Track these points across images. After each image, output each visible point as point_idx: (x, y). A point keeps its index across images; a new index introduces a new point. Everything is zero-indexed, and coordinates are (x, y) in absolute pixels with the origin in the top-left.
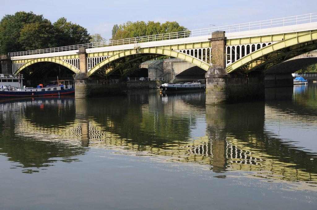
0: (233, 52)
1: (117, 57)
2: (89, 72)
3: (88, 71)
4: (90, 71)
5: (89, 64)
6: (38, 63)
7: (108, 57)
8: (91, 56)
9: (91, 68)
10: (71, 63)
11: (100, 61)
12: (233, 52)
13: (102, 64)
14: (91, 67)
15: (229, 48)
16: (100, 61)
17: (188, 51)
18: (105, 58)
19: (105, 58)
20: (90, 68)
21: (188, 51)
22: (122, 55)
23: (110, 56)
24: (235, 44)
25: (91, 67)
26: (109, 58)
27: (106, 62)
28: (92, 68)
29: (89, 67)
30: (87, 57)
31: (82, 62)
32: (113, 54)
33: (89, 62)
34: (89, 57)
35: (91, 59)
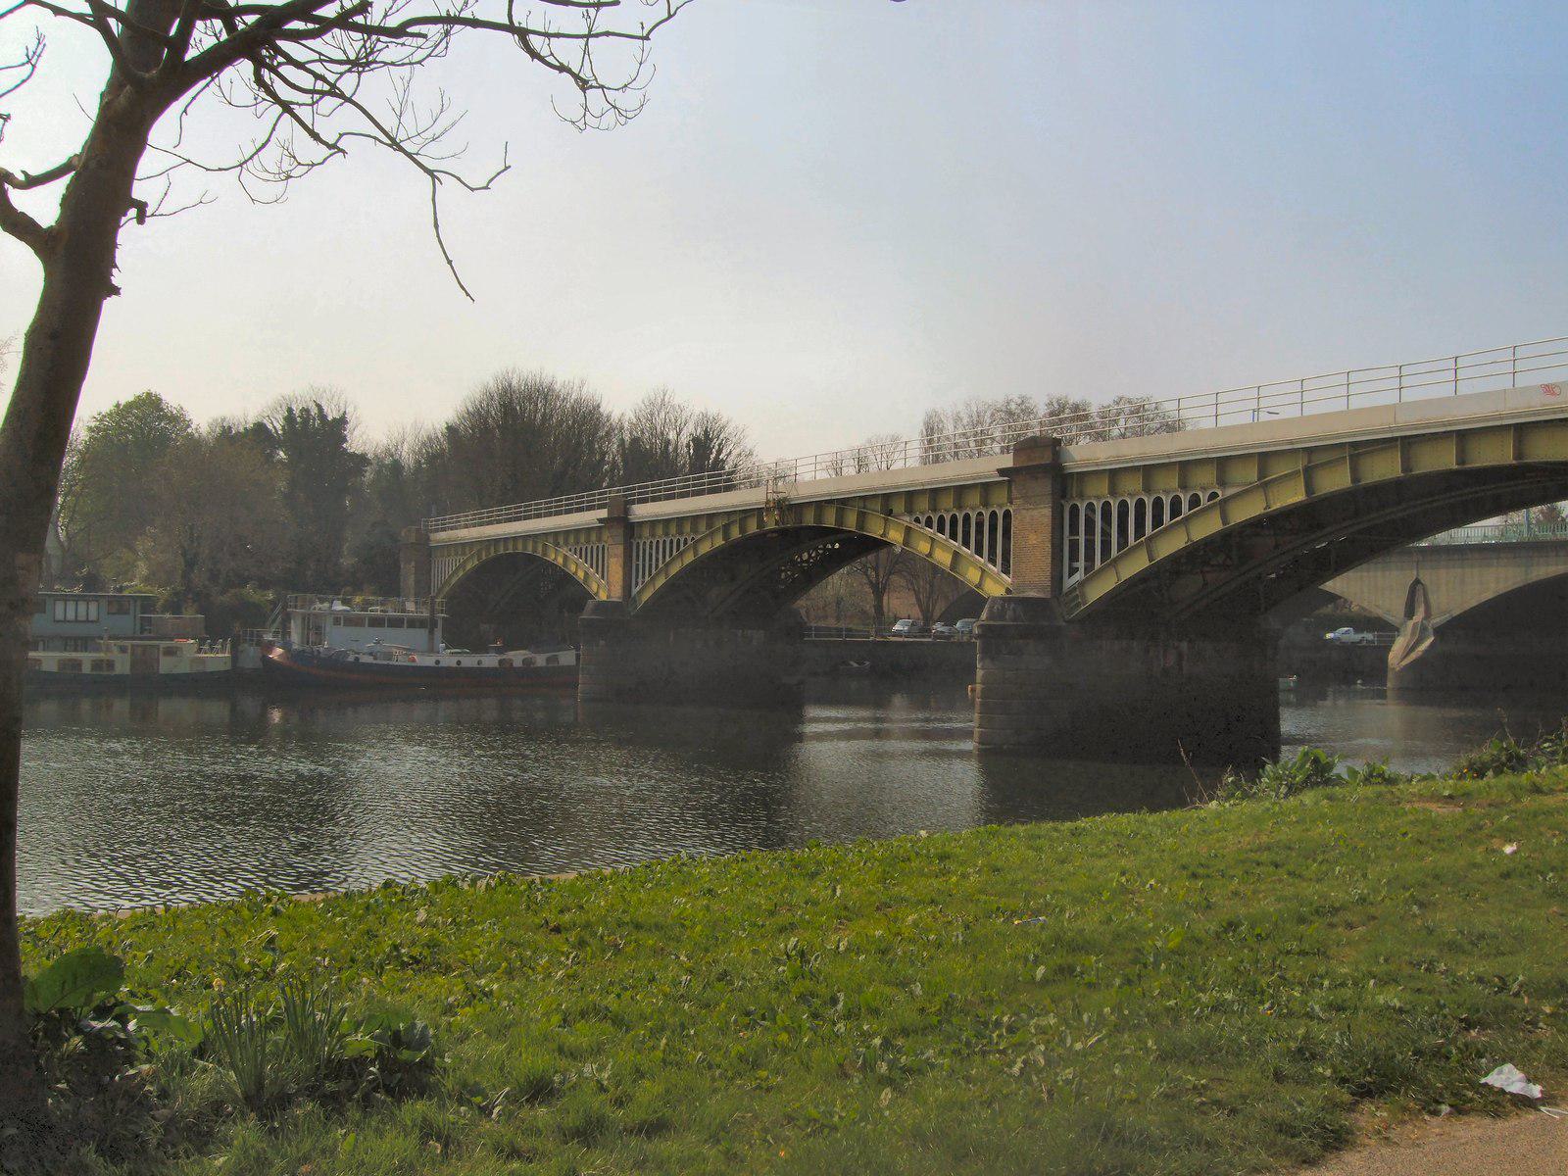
0: (1090, 524)
1: (1293, 495)
2: (1073, 589)
3: (1069, 582)
4: (1082, 584)
5: (1074, 546)
6: (498, 559)
7: (1214, 496)
8: (1098, 493)
9: (1087, 570)
10: (954, 536)
11: (1157, 521)
12: (1090, 524)
13: (1171, 545)
14: (1090, 558)
15: (1075, 510)
16: (1157, 521)
17: (941, 519)
18: (1195, 501)
19: (1195, 501)
20: (1081, 564)
21: (941, 519)
22: (1336, 480)
23: (1230, 492)
24: (1098, 493)
25: (1090, 558)
26: (1226, 501)
27: (1208, 526)
28: (1098, 564)
29: (1074, 557)
30: (632, 536)
31: (616, 556)
32: (1262, 474)
33: (1074, 530)
34: (1081, 496)
35: (1091, 507)
